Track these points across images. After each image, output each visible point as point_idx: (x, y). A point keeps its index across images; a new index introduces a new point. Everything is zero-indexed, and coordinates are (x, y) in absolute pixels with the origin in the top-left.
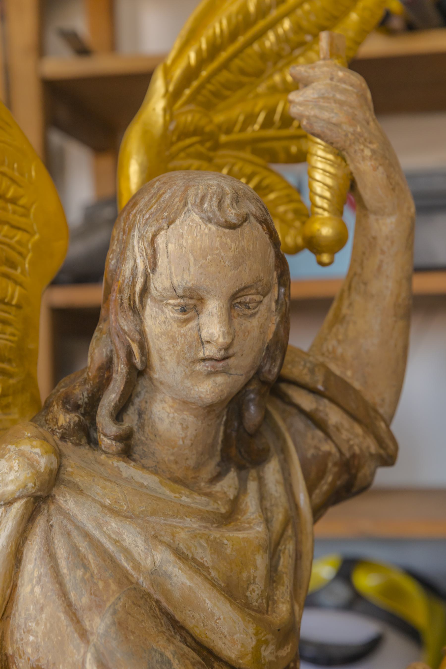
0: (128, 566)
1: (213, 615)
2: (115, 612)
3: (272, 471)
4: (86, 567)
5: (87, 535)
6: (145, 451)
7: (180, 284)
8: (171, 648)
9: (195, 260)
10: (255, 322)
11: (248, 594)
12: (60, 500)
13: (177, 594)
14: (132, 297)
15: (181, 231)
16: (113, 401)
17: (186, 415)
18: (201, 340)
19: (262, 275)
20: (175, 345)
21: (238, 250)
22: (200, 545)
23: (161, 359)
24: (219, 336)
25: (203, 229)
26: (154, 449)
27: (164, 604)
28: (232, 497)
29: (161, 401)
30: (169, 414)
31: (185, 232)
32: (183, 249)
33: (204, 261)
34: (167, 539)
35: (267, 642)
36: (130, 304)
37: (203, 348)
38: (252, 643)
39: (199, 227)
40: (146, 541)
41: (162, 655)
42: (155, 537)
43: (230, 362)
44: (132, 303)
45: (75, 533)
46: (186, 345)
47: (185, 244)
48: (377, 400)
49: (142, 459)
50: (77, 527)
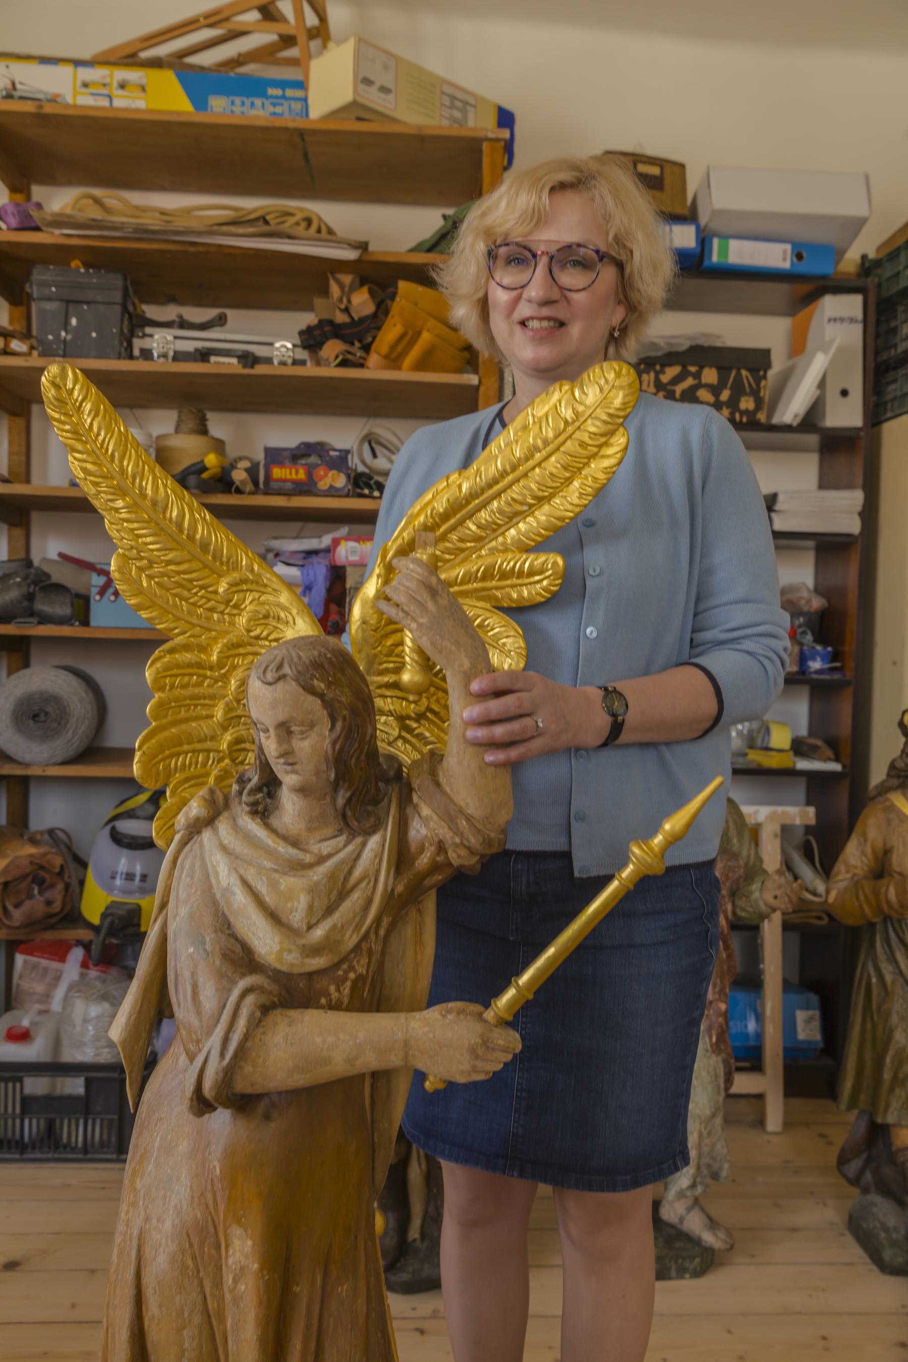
0: (213, 881)
1: (255, 923)
2: (192, 907)
3: (374, 842)
4: (192, 878)
5: (203, 859)
8: (213, 936)
10: (306, 744)
11: (291, 917)
12: (204, 835)
13: (235, 906)
19: (295, 714)
22: (262, 880)
27: (226, 911)
28: (325, 853)
34: (242, 872)
35: (290, 951)
38: (276, 948)
40: (229, 870)
41: (203, 938)
42: (235, 869)
43: (296, 767)
45: (198, 856)
48: (462, 803)
50: (201, 854)
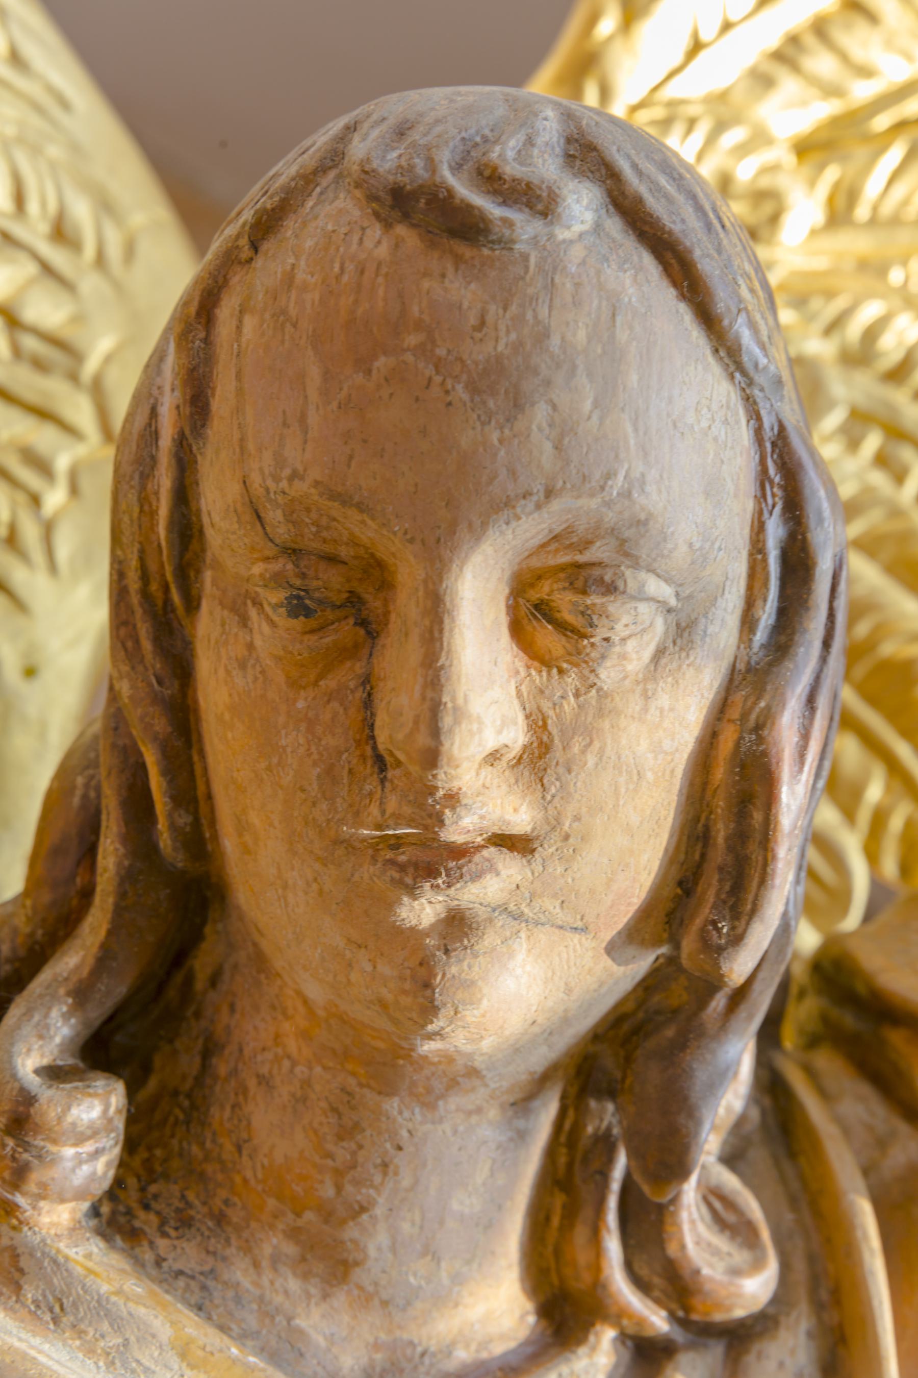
6: (189, 1205)
7: (270, 483)
9: (327, 375)
14: (153, 567)
15: (291, 260)
16: (66, 979)
17: (354, 1074)
18: (375, 748)
20: (275, 760)
21: (513, 336)
23: (242, 827)
24: (416, 722)
25: (369, 243)
26: (226, 1202)
29: (273, 1007)
30: (294, 1063)
31: (303, 263)
32: (289, 328)
33: (359, 378)
36: (145, 594)
37: (383, 781)
39: (356, 238)
44: (154, 587)
46: (315, 764)
47: (293, 311)
49: (165, 1235)
